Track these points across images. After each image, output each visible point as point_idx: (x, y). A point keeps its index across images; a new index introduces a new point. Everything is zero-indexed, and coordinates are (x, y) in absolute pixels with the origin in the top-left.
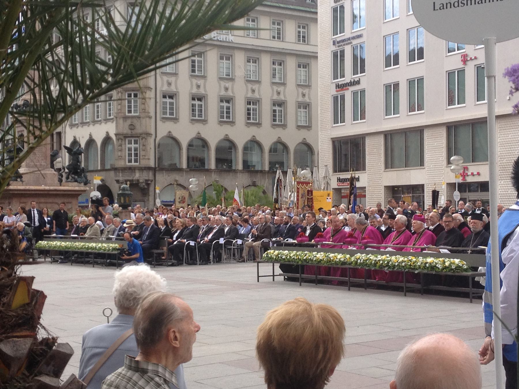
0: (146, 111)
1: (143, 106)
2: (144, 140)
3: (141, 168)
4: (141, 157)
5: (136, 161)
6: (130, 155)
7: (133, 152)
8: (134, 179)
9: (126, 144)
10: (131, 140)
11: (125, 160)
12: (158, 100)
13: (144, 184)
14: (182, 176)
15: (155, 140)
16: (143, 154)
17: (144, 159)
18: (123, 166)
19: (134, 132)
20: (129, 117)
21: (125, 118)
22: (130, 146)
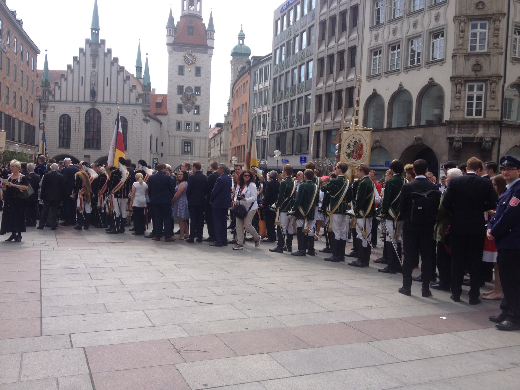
0: (499, 46)
2: (493, 85)
3: (488, 121)
4: (488, 108)
5: (478, 113)
6: (470, 105)
7: (475, 101)
8: (476, 136)
9: (465, 90)
10: (473, 86)
11: (463, 111)
12: (510, 34)
13: (491, 144)
15: (503, 86)
17: (492, 110)
18: (461, 119)
19: (480, 74)
20: (473, 55)
21: (468, 56)
22: (471, 93)
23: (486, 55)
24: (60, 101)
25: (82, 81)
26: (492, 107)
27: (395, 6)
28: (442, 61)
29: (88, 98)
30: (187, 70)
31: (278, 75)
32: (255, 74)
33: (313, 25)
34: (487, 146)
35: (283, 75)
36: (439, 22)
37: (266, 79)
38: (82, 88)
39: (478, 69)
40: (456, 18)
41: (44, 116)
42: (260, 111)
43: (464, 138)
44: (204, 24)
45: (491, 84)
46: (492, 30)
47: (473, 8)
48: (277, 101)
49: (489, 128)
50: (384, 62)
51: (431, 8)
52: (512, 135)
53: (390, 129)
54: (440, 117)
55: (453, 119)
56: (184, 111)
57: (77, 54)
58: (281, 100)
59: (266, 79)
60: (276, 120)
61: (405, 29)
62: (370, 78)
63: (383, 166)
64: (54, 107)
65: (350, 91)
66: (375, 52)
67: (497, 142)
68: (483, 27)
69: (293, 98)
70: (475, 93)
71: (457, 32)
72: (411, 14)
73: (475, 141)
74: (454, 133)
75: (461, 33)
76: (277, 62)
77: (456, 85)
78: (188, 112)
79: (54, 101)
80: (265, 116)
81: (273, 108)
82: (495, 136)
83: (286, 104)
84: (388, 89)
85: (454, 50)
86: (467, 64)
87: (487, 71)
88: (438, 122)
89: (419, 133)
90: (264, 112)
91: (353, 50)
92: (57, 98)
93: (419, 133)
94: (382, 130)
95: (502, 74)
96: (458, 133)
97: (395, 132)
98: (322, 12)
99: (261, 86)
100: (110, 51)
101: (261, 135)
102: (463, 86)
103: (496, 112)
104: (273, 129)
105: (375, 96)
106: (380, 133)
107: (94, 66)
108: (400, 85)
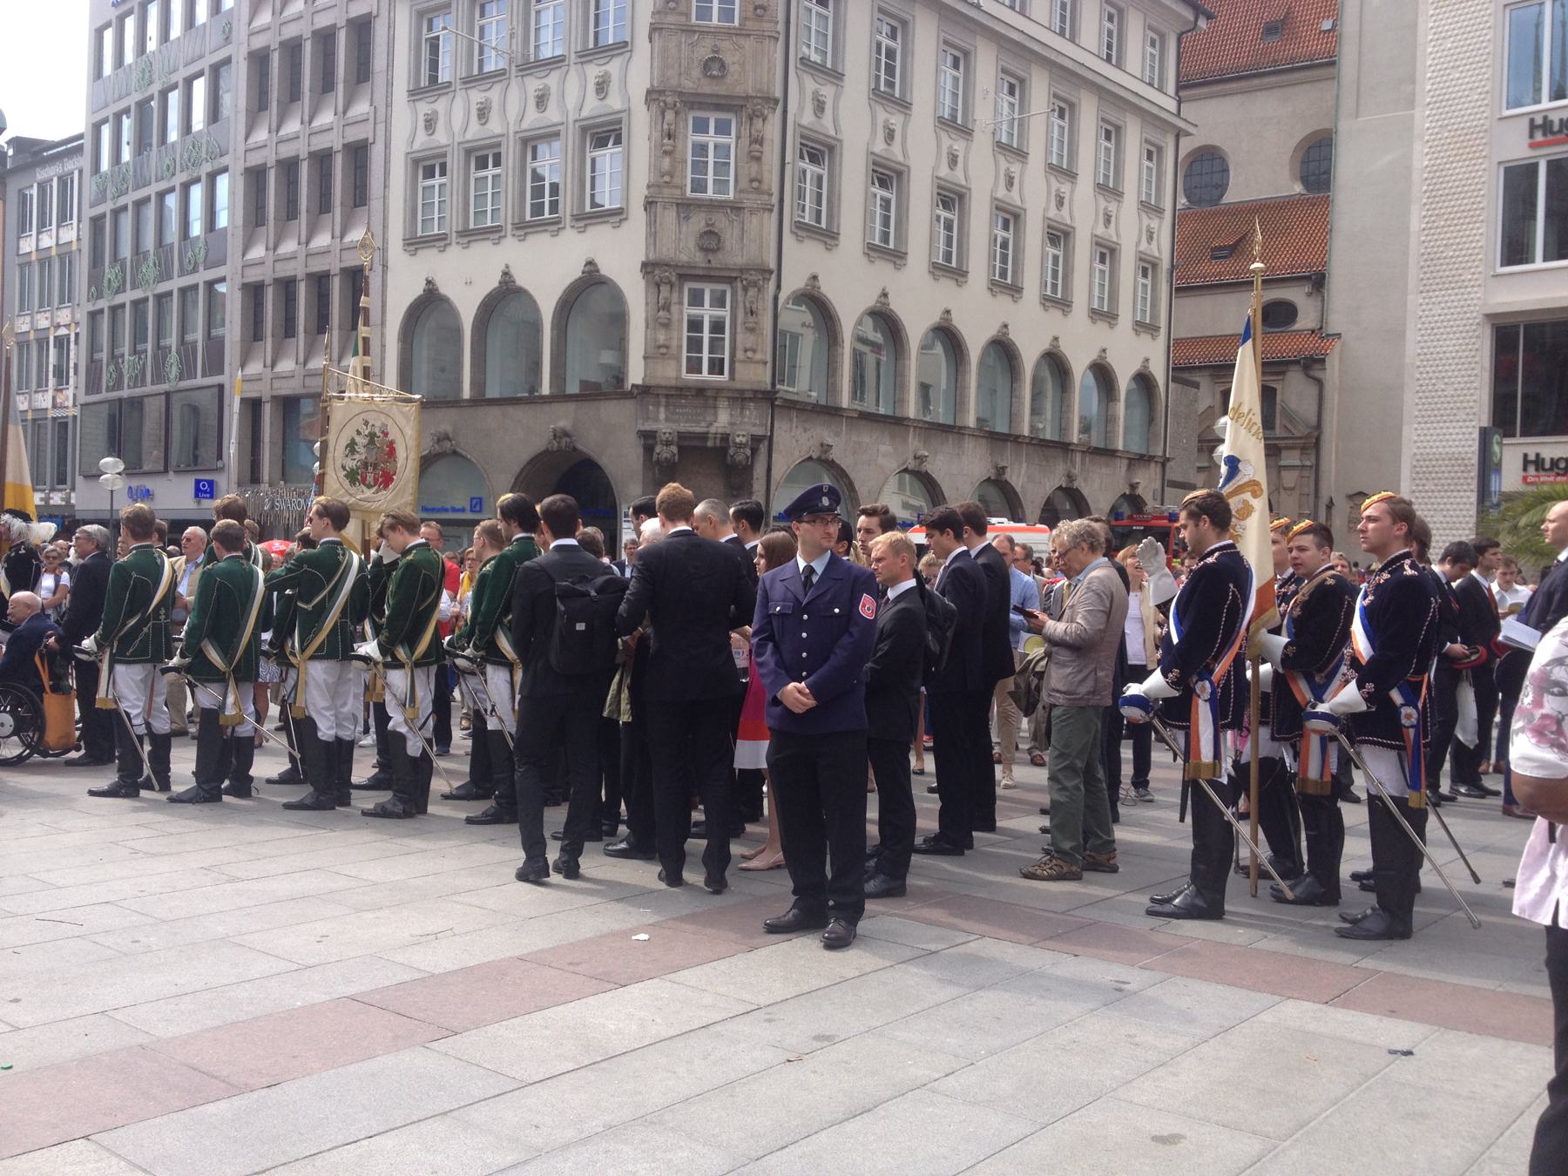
0: (765, 187)
1: (754, 166)
2: (752, 292)
3: (742, 391)
4: (740, 355)
5: (716, 366)
6: (695, 344)
7: (706, 335)
8: (712, 430)
9: (681, 303)
10: (702, 291)
11: (679, 360)
12: (788, 159)
13: (749, 452)
14: (837, 434)
15: (776, 299)
16: (748, 345)
17: (750, 360)
18: (673, 383)
19: (718, 260)
21: (685, 207)
22: (695, 311)
23: (732, 208)
26: (750, 354)
27: (482, 37)
28: (617, 216)
31: (106, 208)
32: (23, 199)
33: (227, 61)
34: (739, 458)
35: (125, 208)
36: (608, 101)
37: (63, 217)
39: (713, 245)
40: (653, 95)
42: (43, 322)
43: (682, 436)
45: (745, 289)
46: (745, 141)
47: (696, 73)
48: (106, 291)
49: (742, 408)
50: (455, 201)
51: (586, 56)
52: (800, 430)
53: (479, 401)
54: (619, 376)
55: (653, 383)
58: (121, 290)
59: (63, 217)
60: (104, 356)
61: (513, 110)
62: (415, 243)
63: (463, 510)
65: (356, 279)
66: (427, 166)
67: (763, 448)
68: (723, 129)
69: (163, 287)
70: (707, 313)
71: (656, 135)
72: (530, 66)
73: (710, 444)
74: (657, 420)
75: (666, 141)
76: (105, 165)
77: (658, 286)
80: (61, 343)
81: (94, 316)
82: (759, 431)
83: (138, 304)
84: (469, 283)
85: (649, 187)
86: (684, 229)
87: (736, 254)
88: (612, 387)
89: (563, 417)
90: (58, 326)
91: (358, 153)
93: (563, 417)
94: (457, 403)
95: (773, 265)
96: (667, 419)
97: (495, 411)
98: (257, 23)
99: (47, 241)
101: (49, 405)
102: (676, 288)
103: (760, 368)
104: (93, 385)
105: (430, 302)
106: (453, 412)
108: (506, 274)
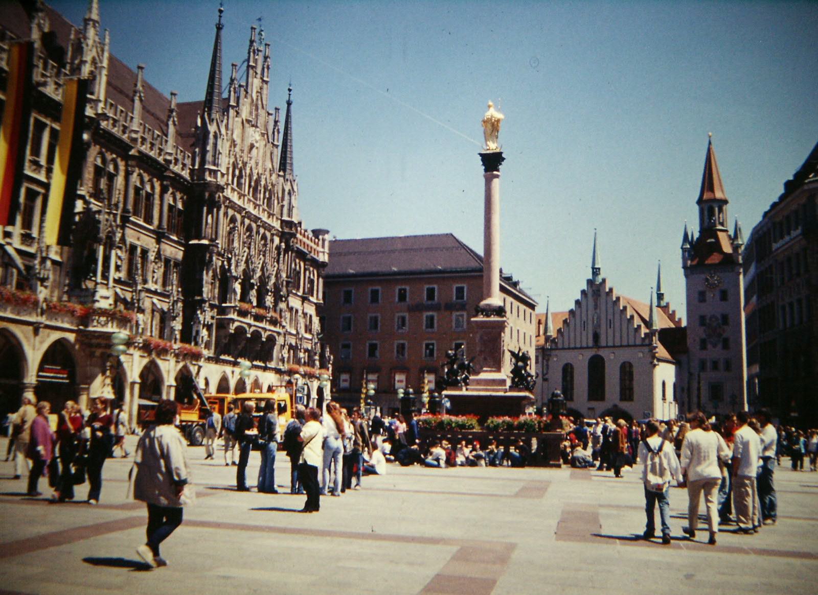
24: (563, 349)
25: (584, 325)
29: (591, 344)
30: (709, 295)
38: (584, 333)
41: (547, 365)
44: (729, 236)
56: (709, 346)
57: (579, 297)
64: (556, 356)
78: (715, 346)
79: (557, 349)
92: (560, 346)
100: (611, 290)
107: (596, 307)
